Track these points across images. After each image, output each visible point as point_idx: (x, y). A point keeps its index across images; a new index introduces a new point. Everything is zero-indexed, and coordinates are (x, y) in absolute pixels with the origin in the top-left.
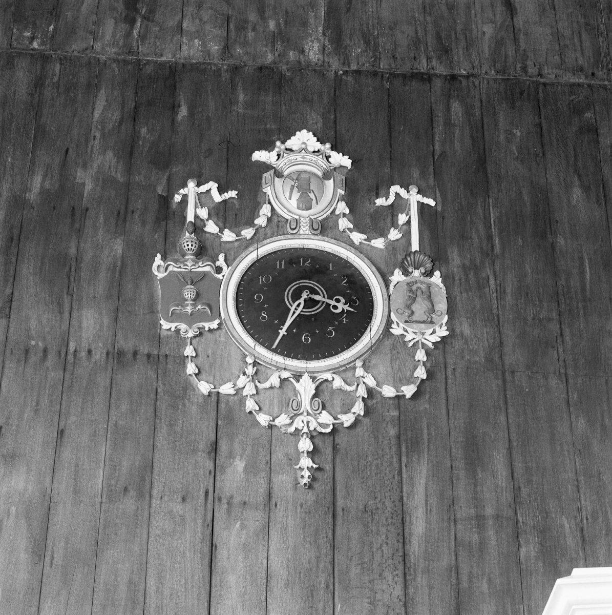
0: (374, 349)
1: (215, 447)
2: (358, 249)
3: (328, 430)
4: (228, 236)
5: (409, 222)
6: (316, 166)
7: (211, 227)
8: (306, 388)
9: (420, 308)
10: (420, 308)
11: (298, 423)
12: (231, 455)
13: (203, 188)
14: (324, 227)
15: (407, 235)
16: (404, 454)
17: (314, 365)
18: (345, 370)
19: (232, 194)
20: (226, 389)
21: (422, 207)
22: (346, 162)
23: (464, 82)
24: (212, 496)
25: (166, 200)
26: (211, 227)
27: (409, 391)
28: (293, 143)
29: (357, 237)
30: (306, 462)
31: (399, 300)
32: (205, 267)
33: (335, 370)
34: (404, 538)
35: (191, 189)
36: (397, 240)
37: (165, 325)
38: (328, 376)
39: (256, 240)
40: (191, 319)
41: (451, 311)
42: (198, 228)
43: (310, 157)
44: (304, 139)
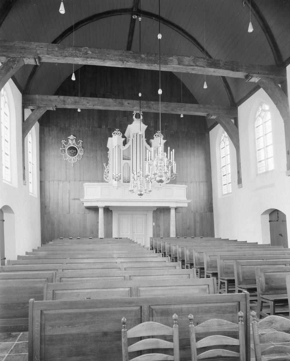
4: (66, 145)
6: (73, 138)
7: (65, 145)
8: (72, 159)
9: (81, 151)
10: (81, 151)
14: (74, 144)
20: (67, 159)
22: (75, 138)
26: (65, 145)
27: (80, 159)
29: (76, 145)
30: (73, 165)
31: (80, 151)
32: (64, 148)
37: (62, 154)
39: (68, 146)
40: (64, 153)
41: (84, 152)
42: (64, 145)
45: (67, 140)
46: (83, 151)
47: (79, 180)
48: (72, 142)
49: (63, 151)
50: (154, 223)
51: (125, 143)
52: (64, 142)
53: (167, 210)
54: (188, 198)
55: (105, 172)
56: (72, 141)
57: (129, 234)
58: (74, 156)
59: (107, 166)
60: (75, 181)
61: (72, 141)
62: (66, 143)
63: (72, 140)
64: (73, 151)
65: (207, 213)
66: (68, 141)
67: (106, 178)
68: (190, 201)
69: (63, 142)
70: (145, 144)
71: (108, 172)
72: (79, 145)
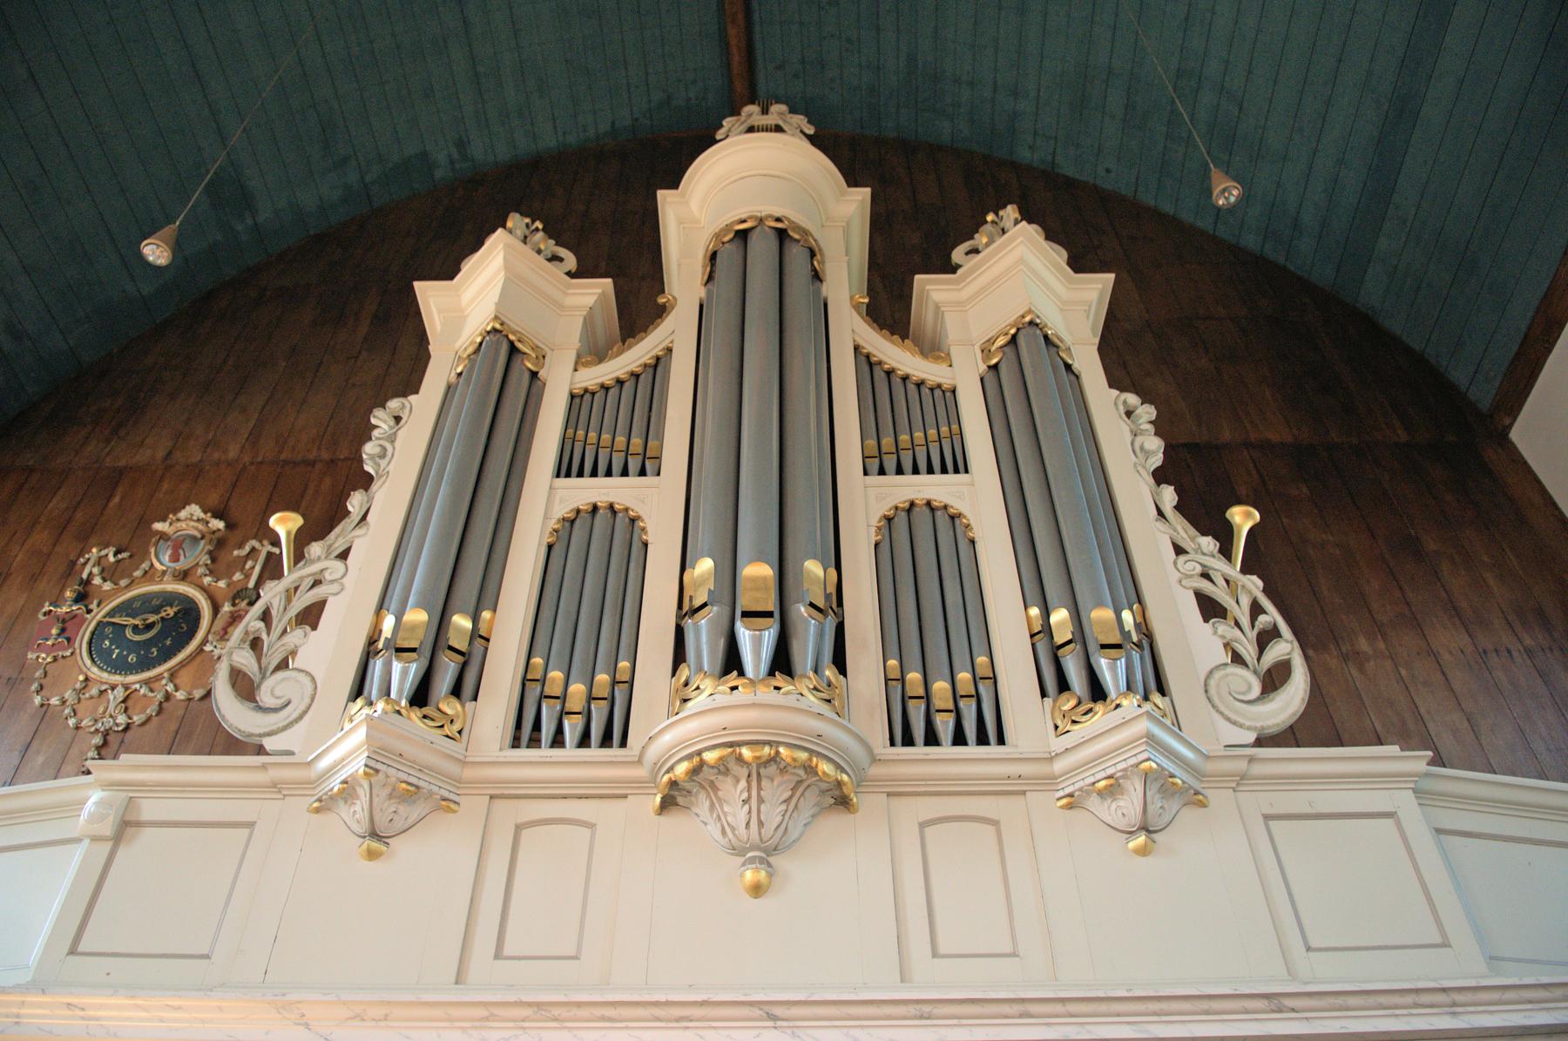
0: (182, 664)
3: (120, 728)
4: (107, 586)
5: (253, 567)
12: (38, 752)
13: (103, 553)
15: (248, 576)
16: (175, 744)
19: (125, 555)
23: (340, 463)
26: (97, 581)
28: (183, 514)
33: (147, 682)
36: (240, 581)
38: (137, 686)
43: (196, 524)
44: (194, 510)
45: (136, 542)
55: (266, 617)
58: (145, 664)
59: (315, 549)
67: (245, 688)
71: (311, 616)
72: (238, 576)
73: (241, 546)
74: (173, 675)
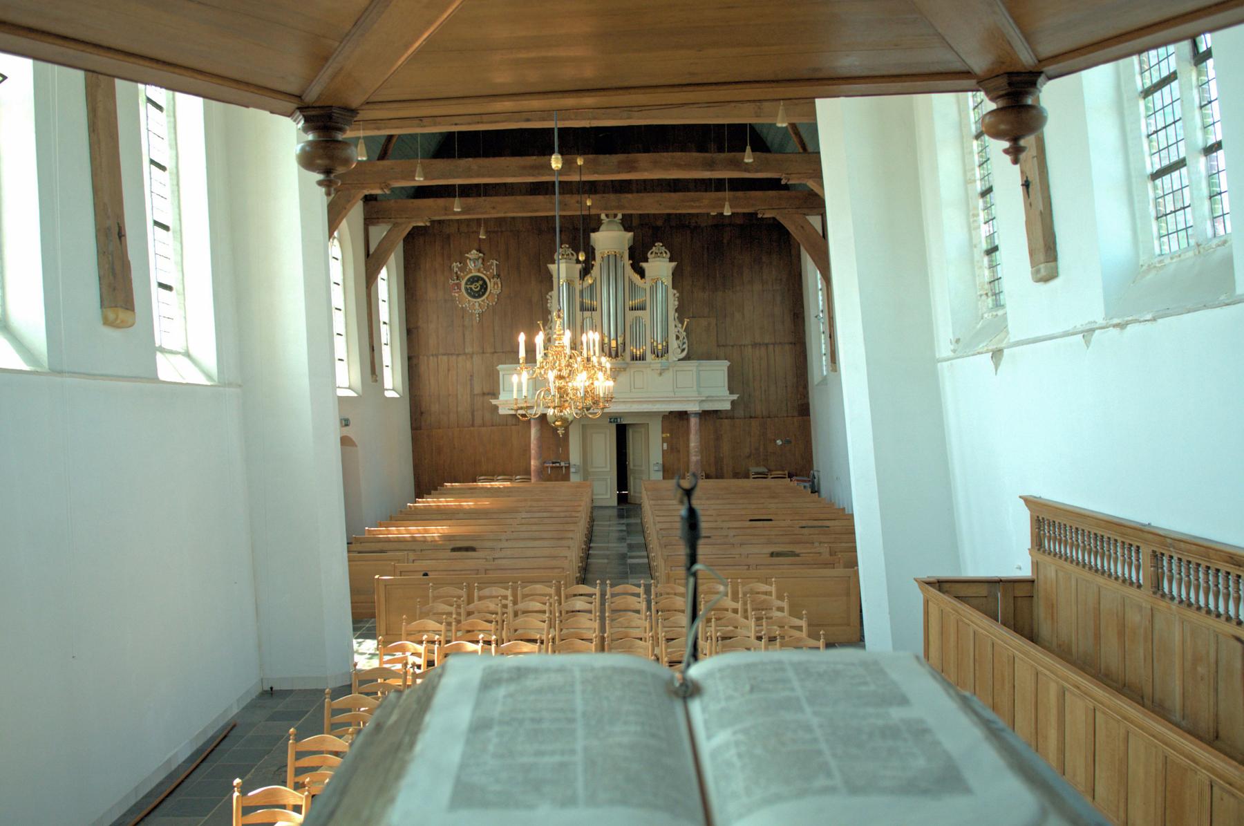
0: (489, 295)
1: (463, 317)
2: (484, 274)
4: (462, 274)
8: (477, 304)
9: (496, 287)
10: (496, 287)
11: (476, 312)
14: (479, 271)
15: (493, 270)
17: (478, 300)
18: (483, 301)
19: (462, 264)
20: (464, 306)
21: (496, 264)
24: (464, 326)
25: (450, 267)
26: (459, 273)
27: (494, 303)
28: (472, 252)
29: (485, 272)
31: (492, 286)
34: (494, 330)
35: (454, 264)
40: (457, 292)
42: (456, 273)
45: (463, 260)
46: (500, 285)
47: (493, 350)
48: (475, 266)
49: (456, 288)
50: (665, 445)
51: (586, 271)
52: (457, 266)
53: (683, 415)
54: (731, 391)
56: (474, 263)
57: (608, 469)
58: (480, 296)
60: (483, 353)
61: (473, 264)
62: (463, 268)
63: (475, 260)
64: (479, 288)
65: (795, 419)
66: (466, 265)
68: (735, 397)
69: (456, 266)
70: (629, 271)
72: (491, 271)
73: (489, 262)
74: (487, 298)
